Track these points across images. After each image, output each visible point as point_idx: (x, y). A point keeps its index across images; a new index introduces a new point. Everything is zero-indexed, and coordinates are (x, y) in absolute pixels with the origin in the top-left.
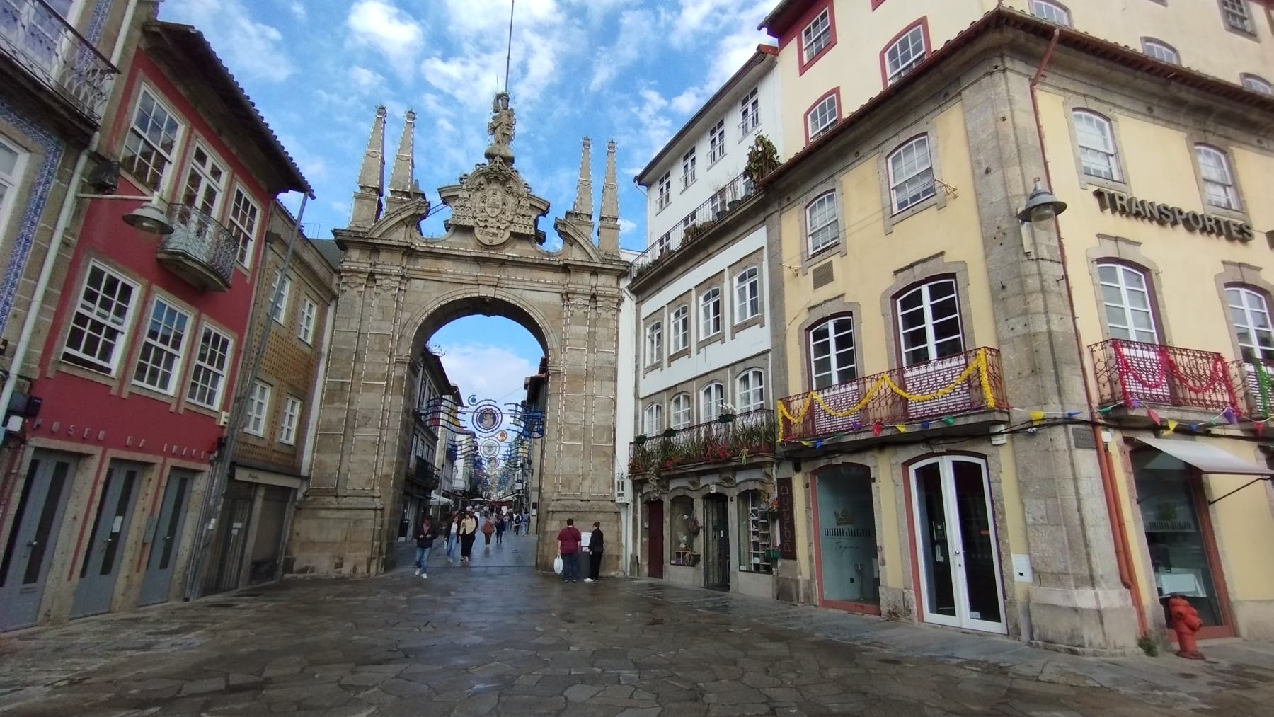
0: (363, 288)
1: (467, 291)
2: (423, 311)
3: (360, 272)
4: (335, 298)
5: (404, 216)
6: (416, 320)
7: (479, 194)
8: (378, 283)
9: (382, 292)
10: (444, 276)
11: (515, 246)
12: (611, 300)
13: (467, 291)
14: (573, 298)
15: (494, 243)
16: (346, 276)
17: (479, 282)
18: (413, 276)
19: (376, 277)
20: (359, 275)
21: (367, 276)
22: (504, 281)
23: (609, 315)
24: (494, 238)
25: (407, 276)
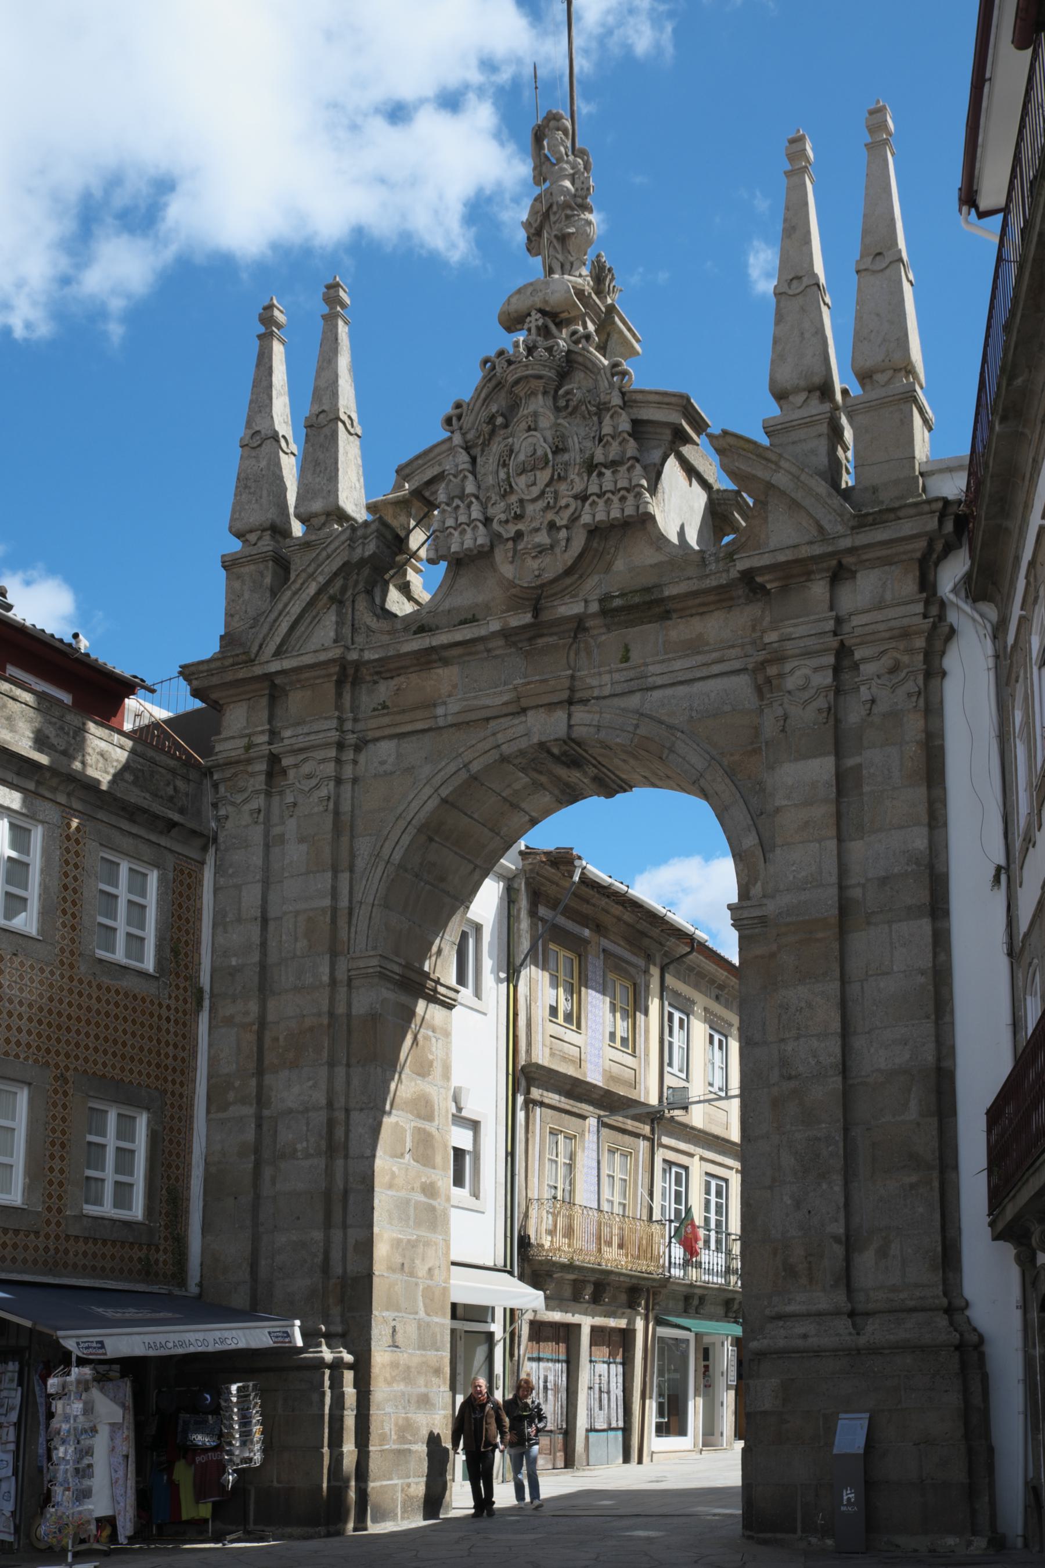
0: (259, 802)
1: (501, 738)
2: (402, 824)
4: (207, 840)
5: (322, 579)
6: (386, 851)
10: (440, 711)
11: (610, 564)
13: (501, 738)
14: (781, 676)
15: (549, 576)
16: (225, 780)
17: (524, 703)
18: (370, 735)
19: (285, 762)
20: (250, 769)
22: (594, 682)
25: (351, 739)
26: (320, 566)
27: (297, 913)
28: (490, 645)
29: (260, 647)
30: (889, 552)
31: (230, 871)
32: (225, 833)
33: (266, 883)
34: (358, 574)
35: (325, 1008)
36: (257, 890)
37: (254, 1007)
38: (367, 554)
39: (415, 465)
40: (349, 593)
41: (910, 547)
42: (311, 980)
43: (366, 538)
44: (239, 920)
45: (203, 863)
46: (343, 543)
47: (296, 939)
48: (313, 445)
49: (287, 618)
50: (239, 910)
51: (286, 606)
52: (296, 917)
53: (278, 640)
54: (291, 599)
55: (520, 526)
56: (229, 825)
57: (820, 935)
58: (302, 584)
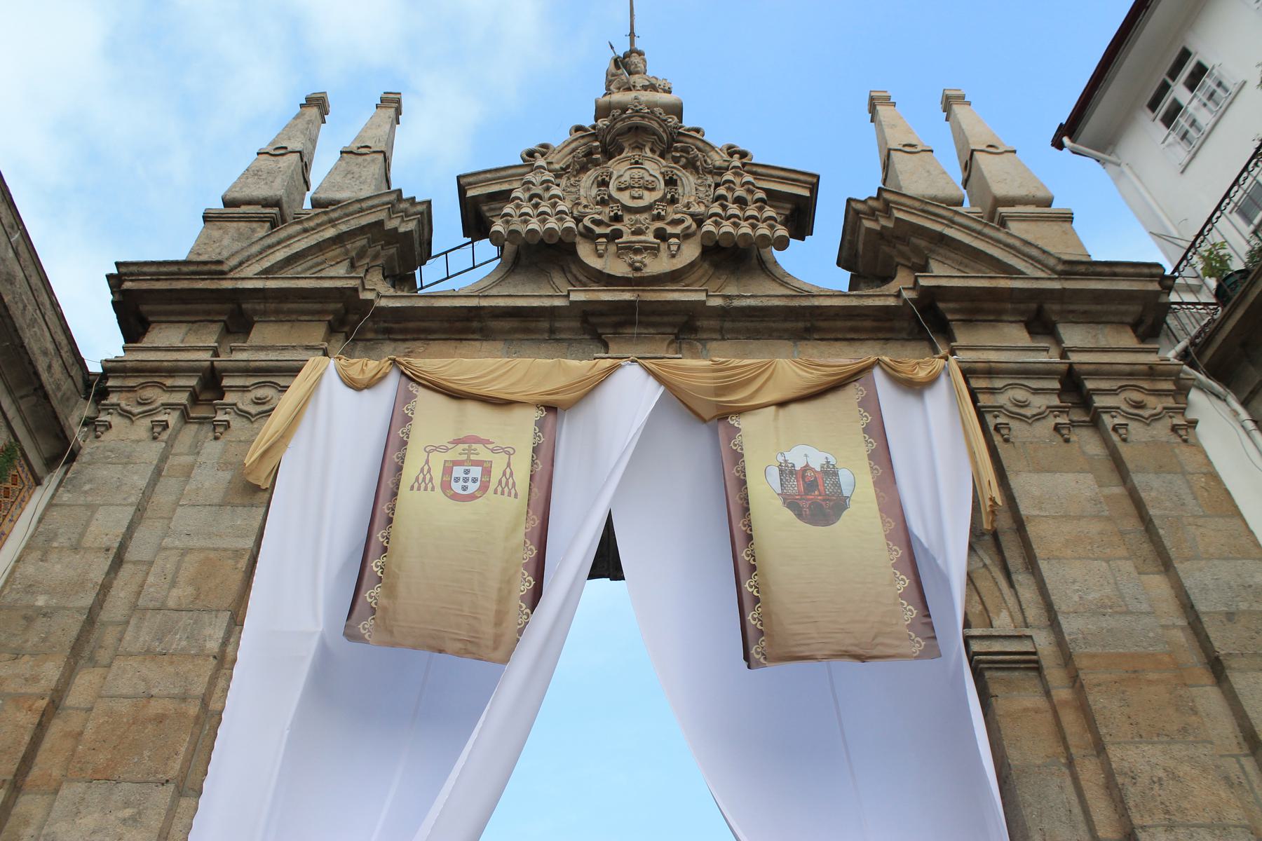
3: (173, 371)
5: (344, 228)
7: (587, 179)
8: (229, 398)
9: (236, 423)
12: (1146, 385)
16: (120, 389)
19: (226, 382)
20: (169, 382)
21: (193, 382)
23: (1161, 430)
24: (648, 260)
26: (347, 215)
27: (185, 552)
28: (557, 325)
29: (241, 264)
30: (1099, 307)
31: (87, 487)
32: (97, 444)
33: (140, 511)
34: (382, 249)
35: (199, 688)
36: (126, 515)
37: (51, 671)
38: (402, 230)
39: (482, 177)
40: (367, 260)
41: (1123, 308)
42: (184, 643)
43: (407, 216)
44: (76, 548)
45: (38, 482)
46: (384, 204)
47: (173, 584)
48: (347, 163)
49: (285, 250)
50: (82, 535)
51: (290, 237)
52: (182, 555)
53: (266, 264)
54: (298, 234)
55: (618, 226)
56: (108, 437)
57: (1152, 676)
58: (319, 225)
